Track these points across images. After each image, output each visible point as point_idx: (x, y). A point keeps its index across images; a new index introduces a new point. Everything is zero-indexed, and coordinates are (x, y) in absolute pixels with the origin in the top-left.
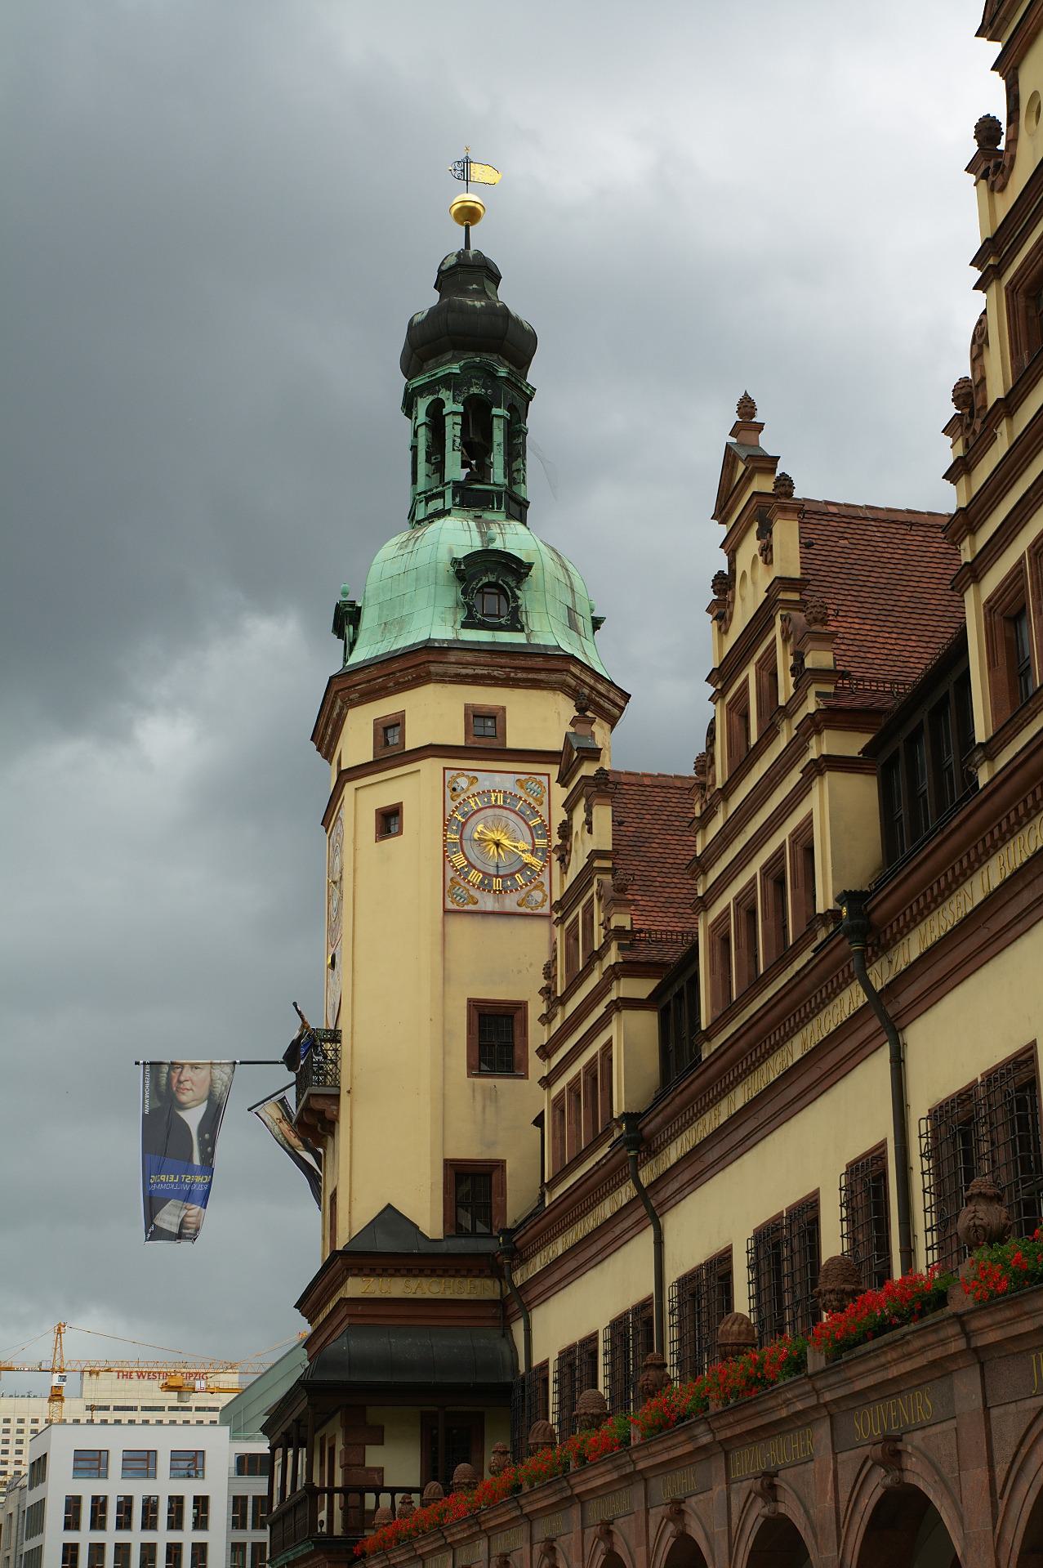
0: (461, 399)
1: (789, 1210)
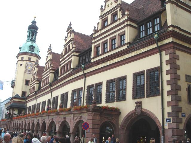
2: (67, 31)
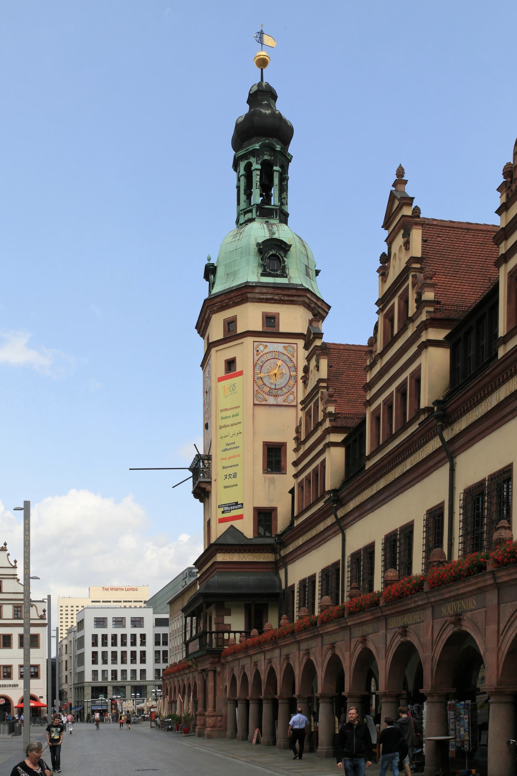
0: (260, 162)
1: (400, 528)
2: (386, 225)
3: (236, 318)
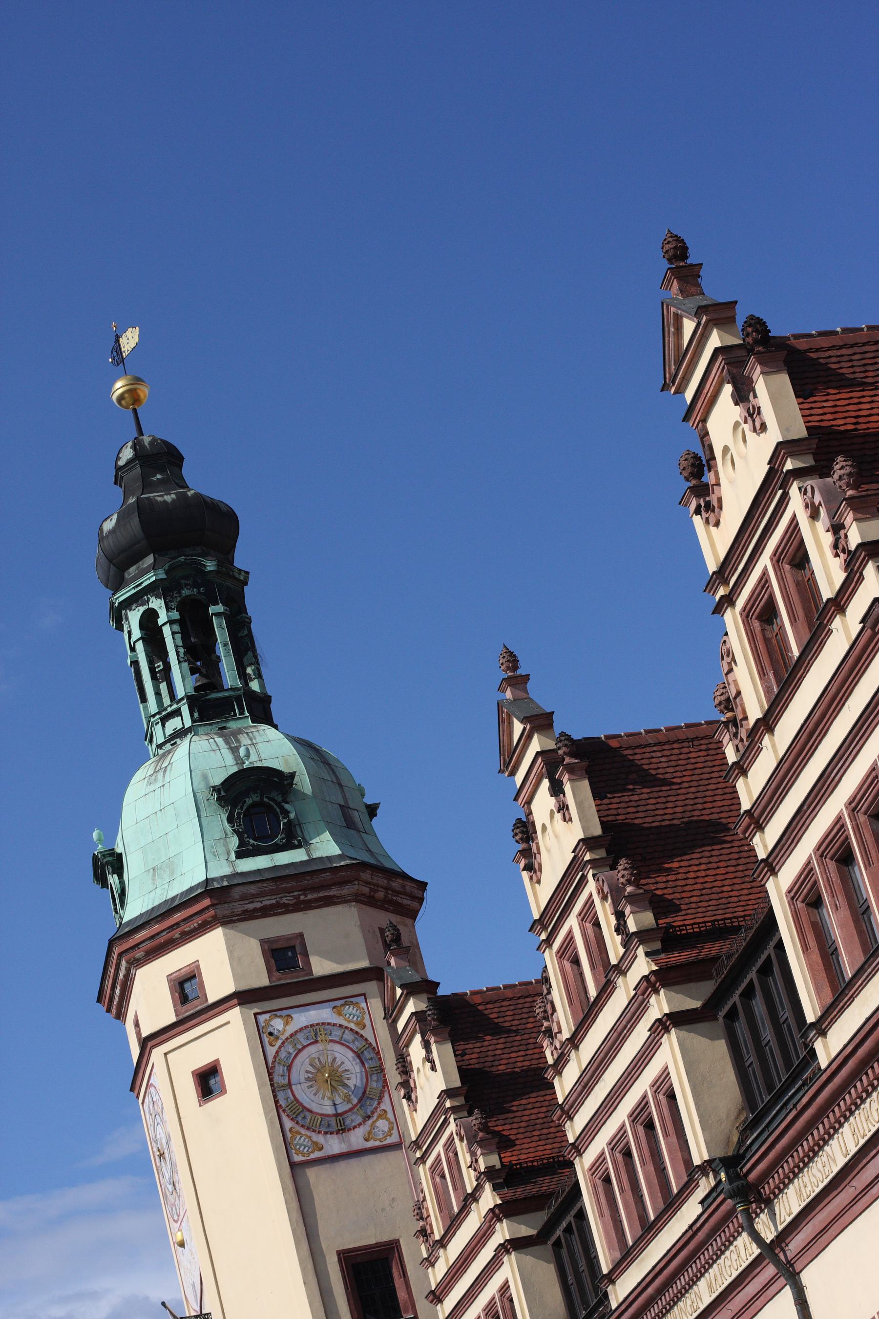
0: (173, 605)
3: (198, 967)
